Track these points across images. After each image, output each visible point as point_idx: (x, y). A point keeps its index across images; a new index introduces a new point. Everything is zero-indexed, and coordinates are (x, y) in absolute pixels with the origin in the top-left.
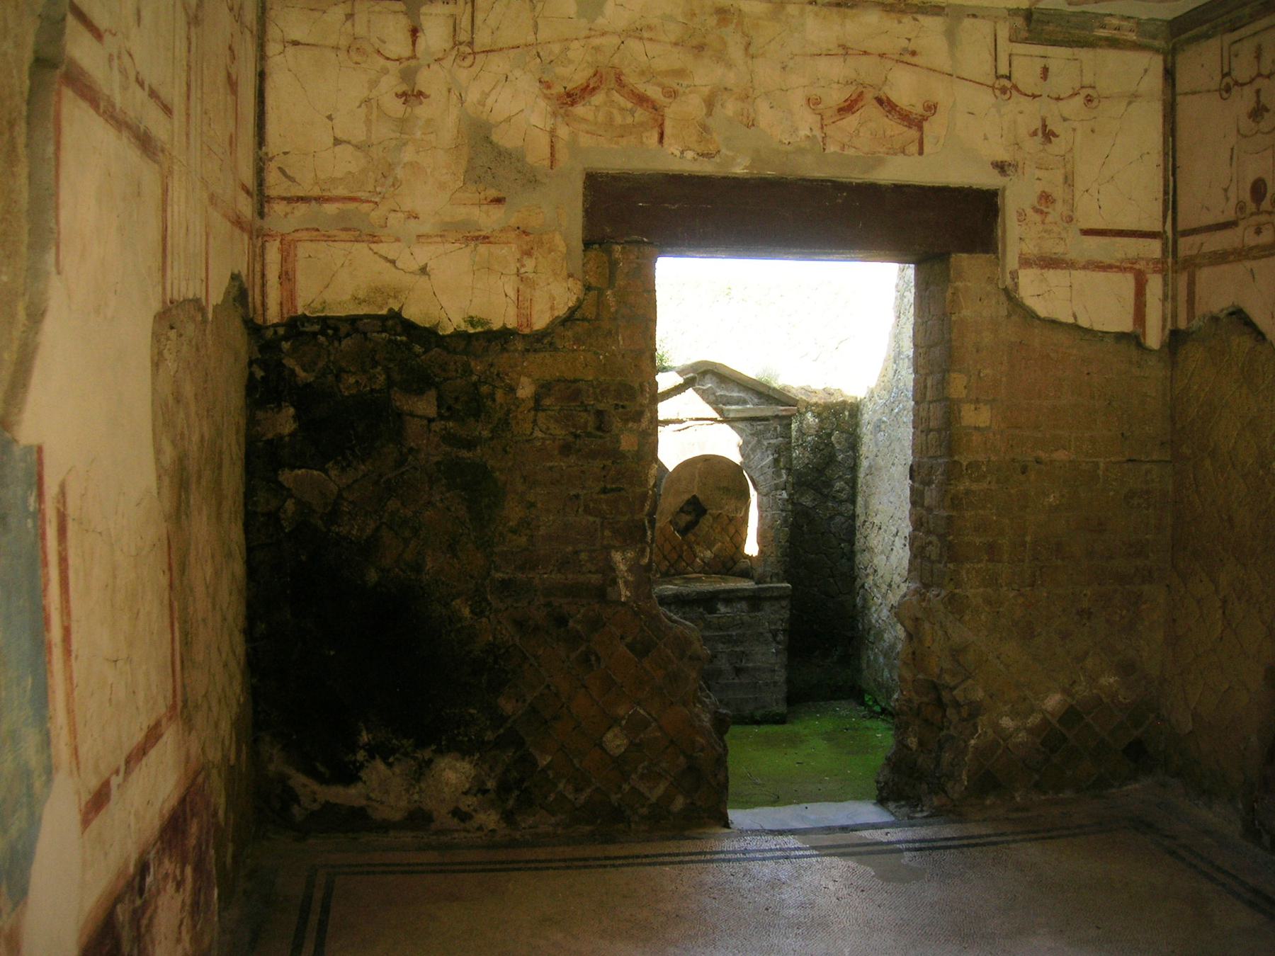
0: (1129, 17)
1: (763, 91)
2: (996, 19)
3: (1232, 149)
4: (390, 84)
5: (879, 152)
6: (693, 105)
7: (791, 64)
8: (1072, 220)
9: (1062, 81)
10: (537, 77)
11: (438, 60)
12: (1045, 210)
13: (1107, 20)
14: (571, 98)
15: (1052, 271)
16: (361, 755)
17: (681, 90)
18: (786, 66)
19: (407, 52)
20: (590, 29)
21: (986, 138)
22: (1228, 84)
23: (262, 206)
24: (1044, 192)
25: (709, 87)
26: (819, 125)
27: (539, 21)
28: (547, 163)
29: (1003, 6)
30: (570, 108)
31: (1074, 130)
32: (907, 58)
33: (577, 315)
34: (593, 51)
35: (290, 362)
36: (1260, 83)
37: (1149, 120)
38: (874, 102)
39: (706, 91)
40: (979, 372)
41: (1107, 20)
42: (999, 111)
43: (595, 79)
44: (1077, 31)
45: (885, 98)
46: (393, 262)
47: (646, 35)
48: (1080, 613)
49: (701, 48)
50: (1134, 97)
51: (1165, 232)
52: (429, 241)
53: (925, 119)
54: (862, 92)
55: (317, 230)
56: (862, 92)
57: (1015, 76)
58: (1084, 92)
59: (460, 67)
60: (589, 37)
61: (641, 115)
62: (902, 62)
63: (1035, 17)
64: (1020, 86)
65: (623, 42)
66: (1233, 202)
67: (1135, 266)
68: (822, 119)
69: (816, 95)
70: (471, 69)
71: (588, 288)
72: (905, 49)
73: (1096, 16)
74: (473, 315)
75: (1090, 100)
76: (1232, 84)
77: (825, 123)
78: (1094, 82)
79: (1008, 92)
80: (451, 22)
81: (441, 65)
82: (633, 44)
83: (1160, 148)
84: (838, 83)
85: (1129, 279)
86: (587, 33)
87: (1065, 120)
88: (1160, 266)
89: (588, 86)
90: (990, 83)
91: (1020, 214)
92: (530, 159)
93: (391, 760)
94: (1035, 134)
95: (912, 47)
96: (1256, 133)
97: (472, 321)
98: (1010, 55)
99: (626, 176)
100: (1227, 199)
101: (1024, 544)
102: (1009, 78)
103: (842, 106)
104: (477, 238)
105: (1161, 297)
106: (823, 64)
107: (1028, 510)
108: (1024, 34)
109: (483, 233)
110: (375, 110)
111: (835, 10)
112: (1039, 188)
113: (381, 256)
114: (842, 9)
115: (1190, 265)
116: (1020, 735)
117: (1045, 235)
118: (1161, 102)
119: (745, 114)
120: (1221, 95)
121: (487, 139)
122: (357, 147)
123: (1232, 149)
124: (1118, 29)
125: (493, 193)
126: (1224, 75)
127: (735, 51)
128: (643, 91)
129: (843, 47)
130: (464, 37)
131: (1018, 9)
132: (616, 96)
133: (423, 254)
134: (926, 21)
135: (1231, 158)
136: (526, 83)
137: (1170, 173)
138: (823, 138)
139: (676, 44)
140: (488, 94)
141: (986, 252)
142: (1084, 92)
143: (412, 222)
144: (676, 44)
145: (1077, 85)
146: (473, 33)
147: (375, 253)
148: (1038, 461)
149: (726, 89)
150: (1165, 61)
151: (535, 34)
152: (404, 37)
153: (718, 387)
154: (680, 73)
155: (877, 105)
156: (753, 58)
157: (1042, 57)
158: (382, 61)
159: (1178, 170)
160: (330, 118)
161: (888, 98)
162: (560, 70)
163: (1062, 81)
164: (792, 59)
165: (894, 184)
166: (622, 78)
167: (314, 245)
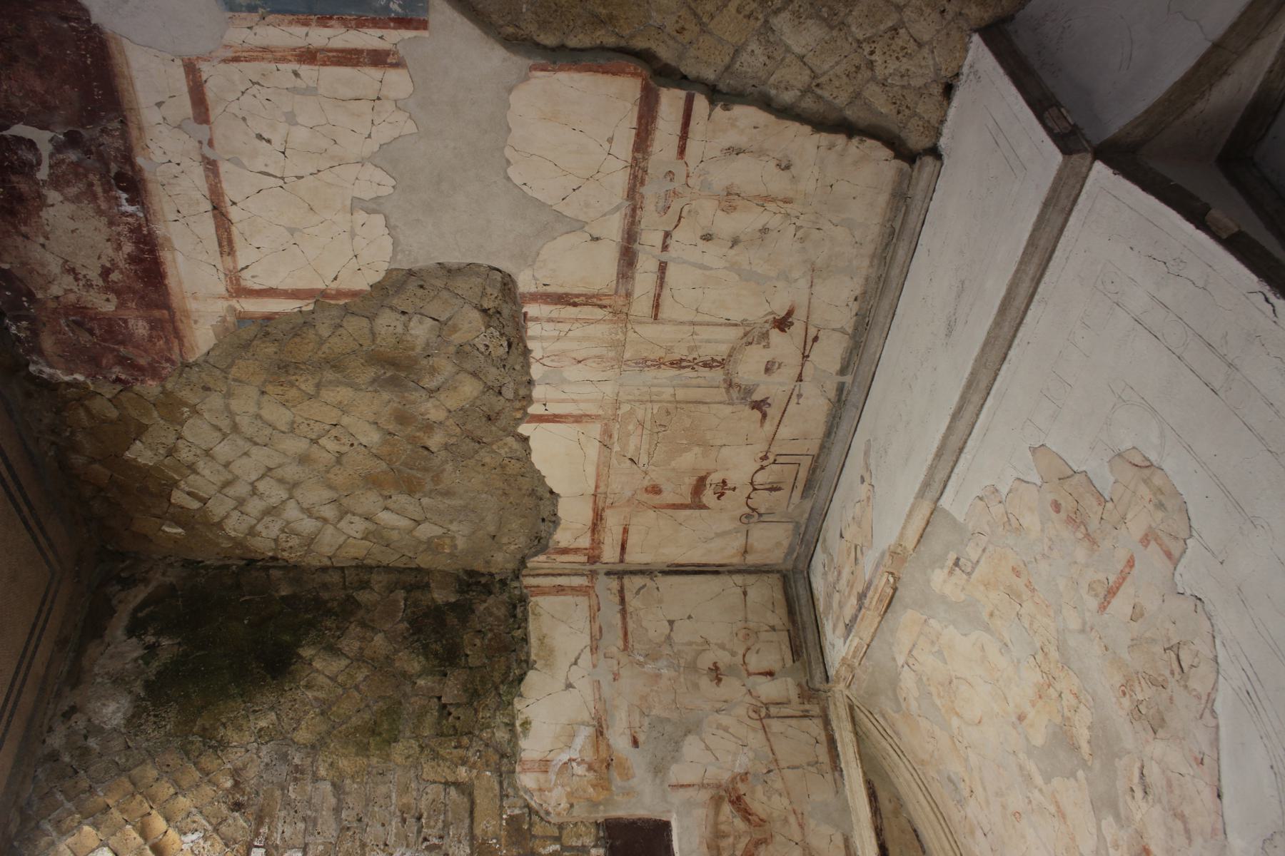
4: (724, 658)
10: (750, 771)
14: (737, 801)
19: (752, 668)
23: (615, 574)
27: (800, 770)
28: (674, 781)
30: (726, 799)
34: (783, 818)
35: (491, 600)
43: (757, 820)
46: (576, 663)
52: (596, 690)
55: (599, 610)
59: (748, 709)
60: (795, 813)
65: (797, 844)
74: (533, 724)
80: (785, 700)
81: (746, 694)
86: (799, 811)
89: (750, 814)
92: (674, 768)
110: (700, 648)
113: (580, 654)
121: (688, 732)
122: (669, 637)
125: (642, 738)
132: (744, 841)
133: (584, 687)
136: (742, 762)
140: (727, 731)
143: (611, 677)
147: (582, 651)
152: (765, 666)
158: (741, 652)
160: (690, 617)
162: (759, 789)
167: (586, 608)
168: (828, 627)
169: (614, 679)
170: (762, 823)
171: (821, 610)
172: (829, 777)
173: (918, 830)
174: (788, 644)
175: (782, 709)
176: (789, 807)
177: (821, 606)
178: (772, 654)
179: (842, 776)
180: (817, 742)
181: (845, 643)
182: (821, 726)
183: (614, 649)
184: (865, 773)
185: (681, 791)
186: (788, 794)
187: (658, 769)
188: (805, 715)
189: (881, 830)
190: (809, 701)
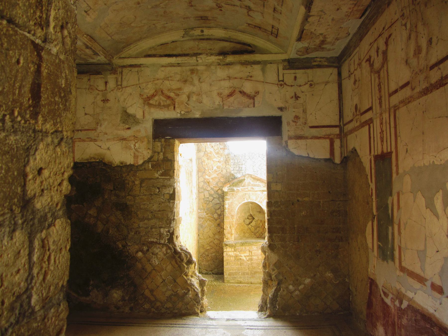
0: (324, 57)
4: (100, 98)
6: (184, 98)
7: (213, 83)
8: (306, 124)
11: (112, 90)
12: (297, 121)
13: (316, 59)
15: (299, 140)
16: (90, 288)
17: (180, 94)
21: (275, 100)
24: (296, 115)
28: (142, 117)
29: (280, 59)
31: (306, 95)
32: (249, 78)
33: (152, 160)
39: (187, 94)
40: (277, 173)
41: (316, 59)
46: (100, 147)
47: (170, 79)
48: (316, 251)
49: (185, 81)
50: (327, 83)
51: (340, 125)
53: (255, 96)
55: (80, 138)
57: (285, 80)
61: (169, 102)
62: (248, 80)
64: (287, 83)
66: (352, 113)
67: (330, 137)
71: (154, 152)
72: (248, 76)
73: (312, 58)
82: (167, 82)
83: (338, 98)
85: (328, 141)
86: (153, 80)
87: (303, 92)
88: (339, 136)
90: (277, 83)
91: (288, 123)
93: (99, 289)
94: (292, 97)
95: (250, 75)
97: (122, 163)
98: (283, 74)
101: (294, 228)
102: (283, 81)
104: (123, 139)
105: (340, 146)
106: (223, 83)
107: (295, 217)
108: (288, 67)
109: (124, 138)
111: (226, 66)
112: (294, 114)
113: (97, 145)
115: (346, 135)
116: (297, 292)
117: (297, 129)
119: (199, 99)
121: (126, 112)
124: (320, 61)
125: (127, 126)
127: (196, 82)
133: (109, 144)
139: (178, 81)
140: (126, 99)
141: (278, 135)
142: (309, 83)
143: (106, 135)
144: (178, 81)
145: (307, 81)
148: (298, 201)
149: (193, 92)
153: (252, 181)
154: (180, 89)
155: (240, 93)
158: (98, 92)
166: (163, 92)
168: (91, 61)
169: (107, 134)
171: (84, 62)
172: (143, 69)
174: (95, 76)
177: (83, 62)
178: (99, 82)
179: (142, 64)
181: (100, 56)
182: (125, 68)
183: (96, 134)
184: (142, 57)
185: (145, 115)
187: (137, 122)
188: (122, 73)
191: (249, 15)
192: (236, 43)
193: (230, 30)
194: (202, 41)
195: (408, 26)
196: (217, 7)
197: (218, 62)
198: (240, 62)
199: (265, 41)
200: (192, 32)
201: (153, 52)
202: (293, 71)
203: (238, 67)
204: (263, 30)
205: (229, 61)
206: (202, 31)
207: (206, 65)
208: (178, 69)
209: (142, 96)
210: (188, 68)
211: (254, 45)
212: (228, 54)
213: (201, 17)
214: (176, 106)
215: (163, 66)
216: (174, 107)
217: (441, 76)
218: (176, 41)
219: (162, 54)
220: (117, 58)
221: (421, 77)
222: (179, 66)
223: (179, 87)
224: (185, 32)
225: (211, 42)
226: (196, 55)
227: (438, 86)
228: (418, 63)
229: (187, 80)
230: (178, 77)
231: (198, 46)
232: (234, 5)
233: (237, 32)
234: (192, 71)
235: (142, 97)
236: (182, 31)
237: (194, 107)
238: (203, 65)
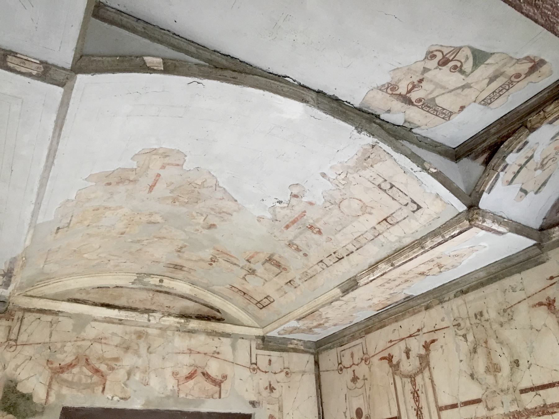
1: (153, 369)
2: (251, 340)
3: (346, 395)
5: (202, 397)
6: (121, 374)
7: (167, 357)
9: (277, 366)
10: (47, 358)
14: (62, 369)
17: (116, 367)
18: (165, 358)
20: (77, 337)
22: (341, 368)
25: (129, 367)
26: (177, 385)
27: (53, 332)
30: (60, 374)
31: (282, 386)
32: (216, 355)
36: (354, 367)
37: (309, 382)
38: (201, 374)
39: (128, 368)
42: (252, 379)
44: (281, 345)
45: (205, 373)
49: (127, 349)
50: (304, 373)
53: (222, 382)
54: (196, 370)
56: (196, 370)
57: (258, 363)
58: (285, 370)
59: (8, 351)
60: (76, 341)
61: (95, 378)
63: (266, 339)
64: (260, 368)
65: (92, 344)
68: (178, 382)
69: (176, 371)
70: (13, 353)
72: (215, 352)
73: (289, 339)
75: (287, 374)
76: (343, 367)
77: (180, 384)
78: (289, 366)
79: (256, 370)
82: (97, 347)
83: (316, 394)
84: (186, 365)
86: (75, 339)
87: (278, 382)
90: (249, 367)
94: (266, 388)
95: (218, 350)
96: (355, 388)
99: (83, 409)
100: (346, 417)
102: (256, 364)
103: (187, 376)
106: (181, 357)
108: (262, 346)
111: (187, 333)
114: (190, 334)
118: (314, 375)
120: (338, 372)
123: (346, 395)
126: (339, 364)
127: (143, 351)
128: (98, 367)
129: (190, 350)
130: (13, 337)
131: (259, 336)
132: (85, 369)
134: (224, 340)
135: (346, 399)
137: (320, 405)
138: (178, 390)
140: (20, 365)
142: (285, 370)
144: (116, 346)
145: (282, 368)
146: (18, 335)
149: (137, 367)
150: (315, 357)
151: (50, 338)
154: (117, 359)
156: (150, 353)
157: (269, 356)
159: (323, 404)
161: (207, 372)
162: (59, 356)
163: (277, 366)
164: (167, 354)
165: (207, 412)
166: (89, 360)
170: (77, 360)
172: (61, 319)
173: (99, 286)
175: (14, 332)
176: (73, 343)
179: (62, 312)
180: (39, 319)
182: (30, 314)
186: (65, 342)
189: (94, 302)
190: (12, 316)
191: (244, 278)
192: (201, 304)
193: (198, 287)
194: (158, 293)
195: (470, 338)
196: (210, 260)
197: (177, 327)
198: (206, 330)
199: (237, 308)
200: (146, 280)
201: (83, 296)
202: (267, 352)
203: (202, 338)
204: (247, 297)
205: (192, 327)
206: (161, 281)
207: (160, 329)
208: (118, 329)
209: (52, 364)
210: (133, 329)
211: (223, 311)
212: (191, 317)
213: (176, 265)
214: (107, 387)
215: (95, 320)
216: (104, 389)
217: (543, 403)
218: (122, 287)
219: (97, 301)
220: (21, 295)
221: (507, 399)
222: (120, 324)
223: (115, 356)
224: (137, 276)
225: (170, 298)
226: (147, 311)
227: (540, 413)
228: (496, 382)
229: (130, 347)
230: (117, 340)
231: (152, 299)
232: (235, 264)
233: (206, 291)
234: (140, 335)
235: (51, 366)
236: (135, 274)
237: (135, 391)
238: (156, 328)
